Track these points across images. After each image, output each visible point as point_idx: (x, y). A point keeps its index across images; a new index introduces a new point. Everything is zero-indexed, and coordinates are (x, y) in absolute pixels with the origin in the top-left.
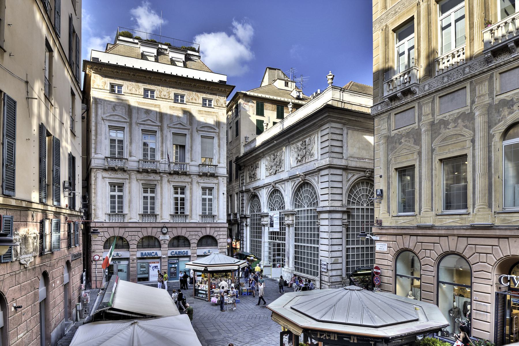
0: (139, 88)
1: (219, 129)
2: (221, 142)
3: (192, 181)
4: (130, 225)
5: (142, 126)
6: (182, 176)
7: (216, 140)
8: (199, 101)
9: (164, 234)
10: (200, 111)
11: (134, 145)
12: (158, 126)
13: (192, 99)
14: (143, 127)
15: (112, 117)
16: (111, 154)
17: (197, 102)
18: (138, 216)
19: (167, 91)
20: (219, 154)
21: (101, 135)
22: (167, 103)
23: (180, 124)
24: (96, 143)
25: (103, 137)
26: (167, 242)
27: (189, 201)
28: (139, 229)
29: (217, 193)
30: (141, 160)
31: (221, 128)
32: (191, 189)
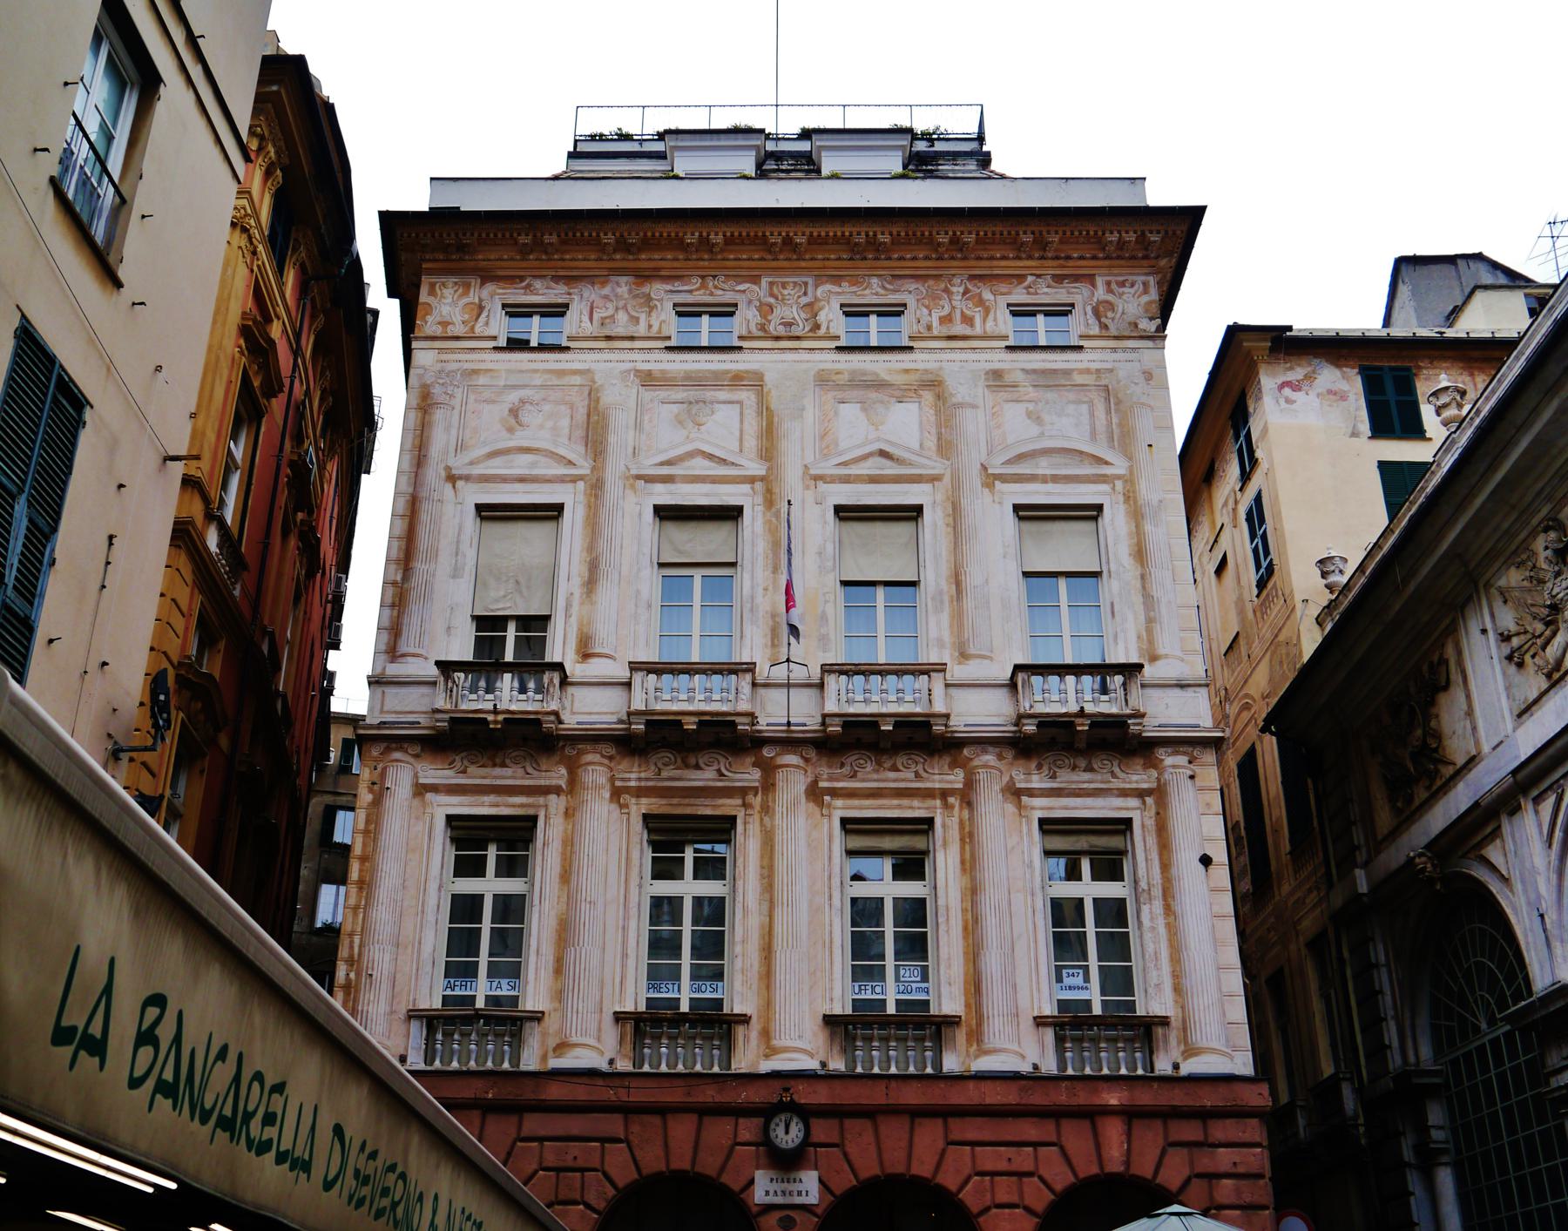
0: (651, 309)
1: (1130, 458)
2: (1148, 527)
3: (970, 784)
4: (555, 1092)
5: (659, 487)
7: (1115, 520)
8: (990, 324)
9: (786, 1163)
10: (997, 374)
11: (607, 594)
12: (751, 480)
13: (946, 320)
15: (497, 461)
17: (978, 330)
18: (611, 1034)
19: (804, 300)
20: (1148, 600)
21: (434, 554)
23: (883, 454)
25: (445, 562)
28: (613, 1125)
29: (1155, 856)
31: (1142, 454)
32: (969, 837)
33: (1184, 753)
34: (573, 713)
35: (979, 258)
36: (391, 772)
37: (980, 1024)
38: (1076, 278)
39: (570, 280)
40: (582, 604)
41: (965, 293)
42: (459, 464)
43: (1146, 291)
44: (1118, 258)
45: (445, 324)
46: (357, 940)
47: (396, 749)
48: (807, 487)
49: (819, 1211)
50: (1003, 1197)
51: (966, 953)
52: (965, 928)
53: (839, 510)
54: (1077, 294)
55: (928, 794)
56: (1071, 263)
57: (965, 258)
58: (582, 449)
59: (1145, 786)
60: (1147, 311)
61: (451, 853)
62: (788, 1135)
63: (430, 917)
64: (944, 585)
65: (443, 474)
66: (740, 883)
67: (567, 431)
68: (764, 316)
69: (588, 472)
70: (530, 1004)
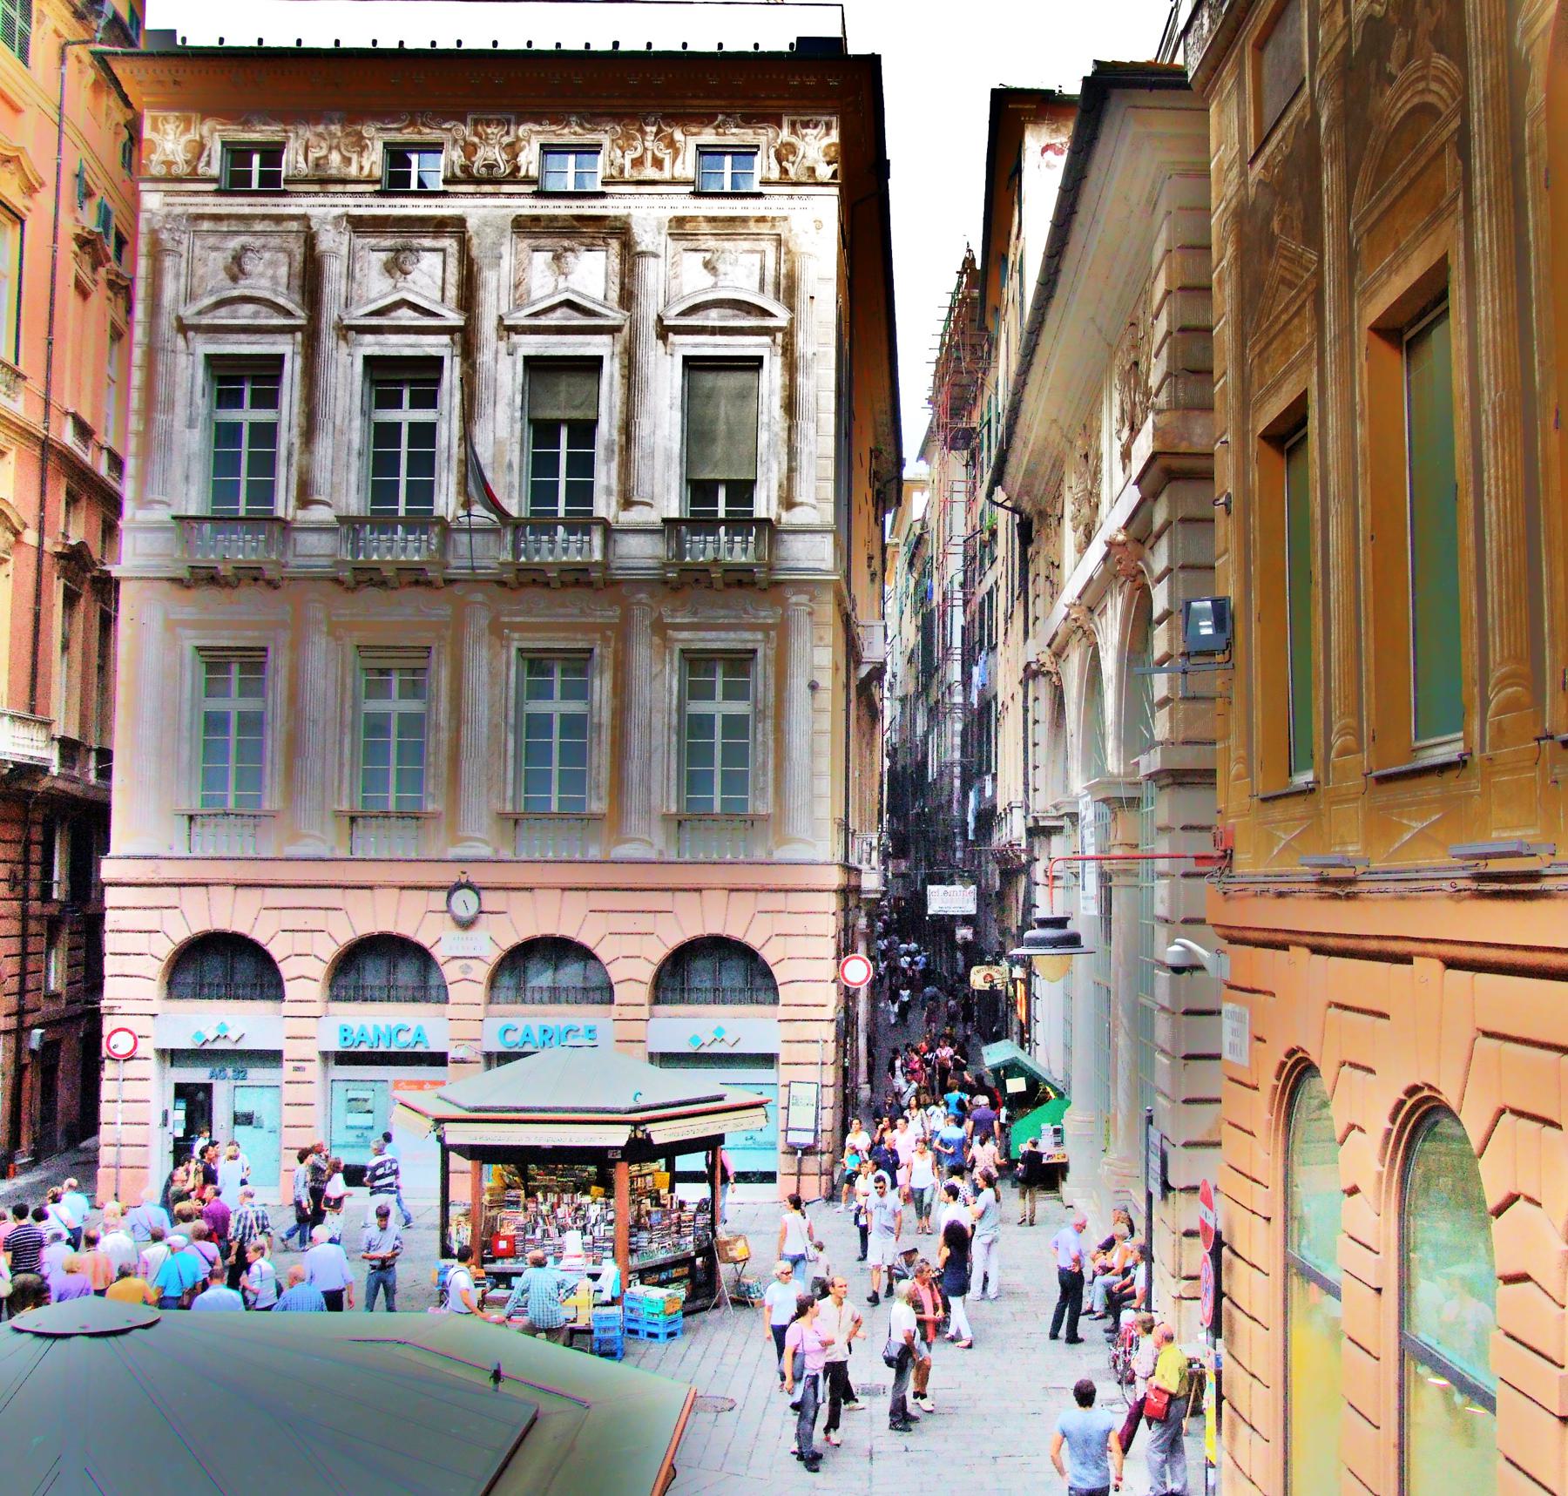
0: (363, 148)
1: (792, 308)
2: (800, 379)
5: (369, 338)
7: (772, 377)
9: (466, 925)
10: (680, 221)
11: (324, 447)
13: (638, 163)
14: (372, 345)
15: (223, 311)
17: (666, 175)
19: (506, 140)
20: (792, 453)
21: (170, 405)
22: (503, 201)
23: (569, 304)
25: (181, 413)
27: (606, 735)
29: (772, 682)
33: (806, 593)
34: (295, 556)
40: (302, 453)
41: (657, 134)
42: (188, 313)
48: (500, 338)
54: (763, 137)
55: (594, 628)
58: (297, 298)
60: (826, 155)
64: (616, 436)
67: (284, 280)
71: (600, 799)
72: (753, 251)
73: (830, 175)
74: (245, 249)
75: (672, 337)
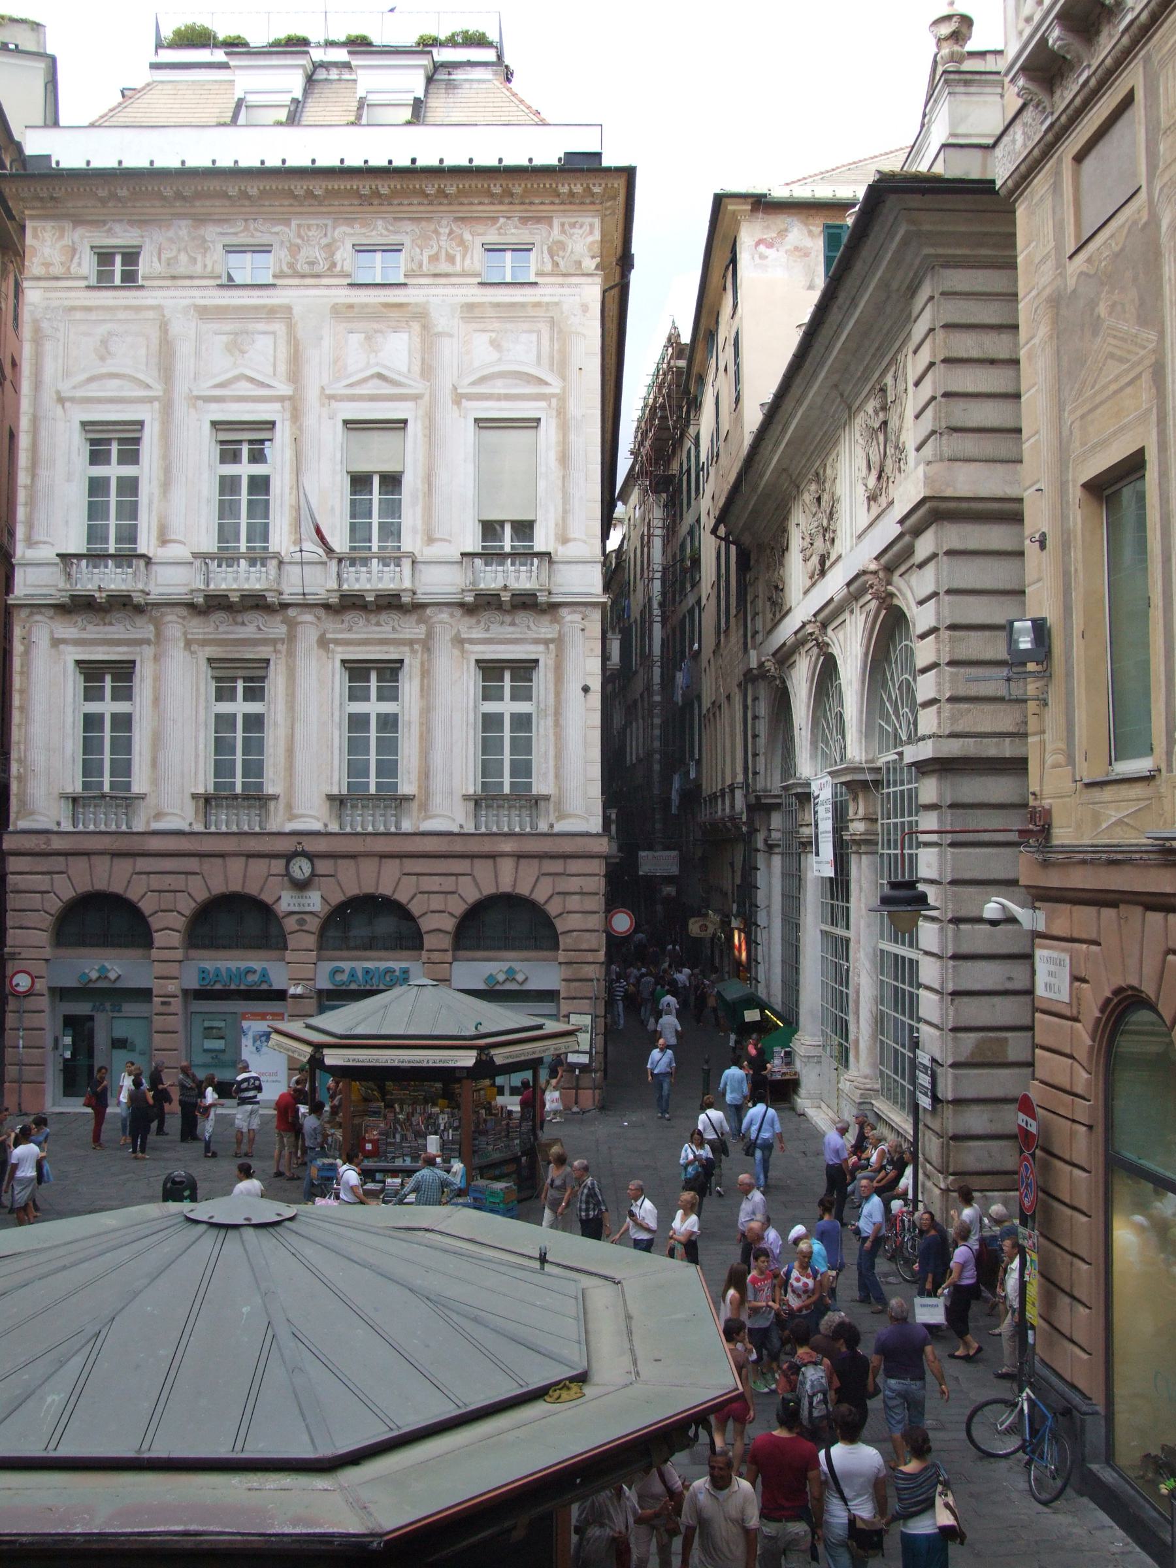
0: (206, 250)
1: (564, 378)
2: (572, 437)
3: (430, 635)
4: (155, 844)
5: (214, 406)
6: (383, 617)
7: (548, 432)
8: (468, 262)
9: (301, 886)
10: (470, 307)
11: (179, 494)
12: (281, 399)
13: (434, 258)
15: (94, 385)
16: (89, 542)
17: (458, 268)
18: (190, 808)
19: (324, 241)
23: (380, 376)
24: (31, 502)
26: (314, 924)
27: (415, 730)
28: (192, 864)
29: (551, 686)
30: (204, 557)
32: (426, 673)
33: (580, 612)
34: (157, 585)
35: (462, 204)
36: (34, 629)
37: (427, 799)
38: (538, 220)
39: (142, 223)
41: (450, 233)
42: (66, 388)
43: (591, 233)
44: (571, 203)
45: (47, 265)
46: (22, 747)
47: (37, 613)
48: (323, 405)
49: (321, 915)
50: (432, 908)
51: (420, 752)
52: (421, 736)
53: (346, 422)
56: (534, 208)
57: (450, 204)
58: (155, 374)
59: (549, 636)
60: (590, 250)
61: (81, 684)
62: (301, 869)
63: (69, 730)
65: (55, 397)
66: (272, 706)
68: (293, 256)
69: (160, 393)
70: (136, 789)
71: (410, 783)
72: (530, 332)
73: (593, 267)
74: (110, 334)
75: (465, 403)
